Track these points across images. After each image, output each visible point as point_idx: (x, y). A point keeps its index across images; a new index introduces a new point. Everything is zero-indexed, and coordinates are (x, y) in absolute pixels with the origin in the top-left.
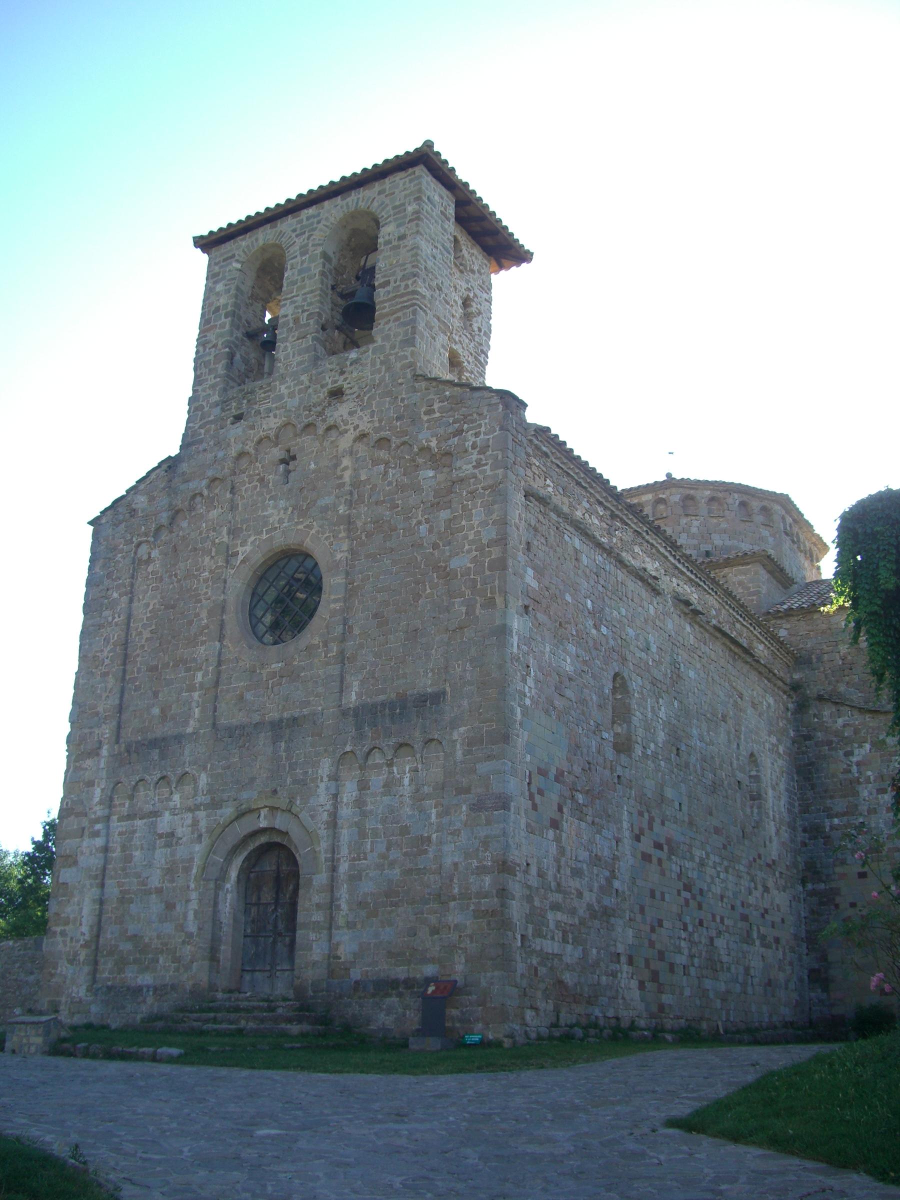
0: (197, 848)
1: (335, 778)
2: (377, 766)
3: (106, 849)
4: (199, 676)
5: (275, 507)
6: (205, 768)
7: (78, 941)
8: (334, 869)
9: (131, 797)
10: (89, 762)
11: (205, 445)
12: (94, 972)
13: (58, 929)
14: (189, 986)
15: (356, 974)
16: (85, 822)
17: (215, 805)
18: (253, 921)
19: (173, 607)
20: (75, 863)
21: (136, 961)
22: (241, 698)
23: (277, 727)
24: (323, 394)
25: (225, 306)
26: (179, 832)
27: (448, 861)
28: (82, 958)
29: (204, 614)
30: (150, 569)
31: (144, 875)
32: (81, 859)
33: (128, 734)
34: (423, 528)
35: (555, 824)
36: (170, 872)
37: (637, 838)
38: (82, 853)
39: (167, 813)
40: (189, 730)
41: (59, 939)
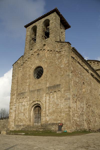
0: (28, 106)
1: (46, 96)
2: (51, 95)
3: (16, 107)
4: (27, 84)
5: (37, 61)
6: (28, 96)
8: (46, 109)
9: (19, 100)
10: (13, 96)
12: (15, 123)
14: (27, 125)
15: (49, 123)
16: (13, 104)
17: (30, 101)
18: (35, 116)
19: (24, 75)
20: (12, 109)
21: (20, 122)
22: (33, 87)
23: (38, 90)
25: (29, 35)
27: (61, 107)
28: (13, 121)
29: (28, 76)
32: (13, 109)
33: (18, 92)
34: (57, 62)
35: (76, 102)
36: (24, 110)
37: (86, 104)
40: (26, 91)
41: (10, 119)
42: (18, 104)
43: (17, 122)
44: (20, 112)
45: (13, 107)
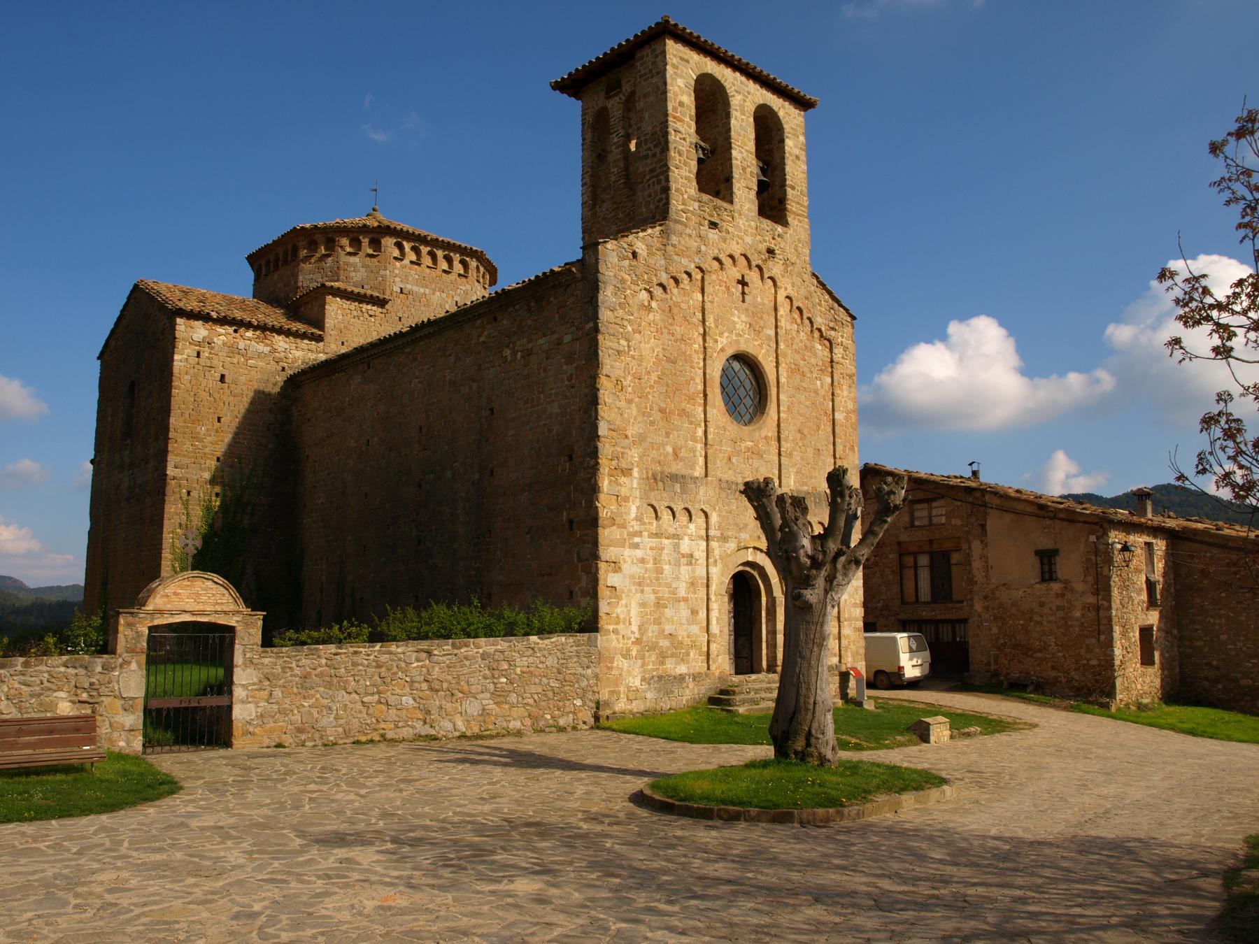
3: (643, 561)
7: (629, 638)
11: (688, 231)
13: (611, 627)
17: (724, 539)
21: (672, 656)
24: (763, 247)
26: (696, 555)
28: (634, 653)
30: (651, 317)
31: (674, 585)
32: (625, 567)
38: (625, 561)
39: (686, 538)
42: (654, 542)
43: (653, 658)
44: (664, 592)
45: (627, 552)
